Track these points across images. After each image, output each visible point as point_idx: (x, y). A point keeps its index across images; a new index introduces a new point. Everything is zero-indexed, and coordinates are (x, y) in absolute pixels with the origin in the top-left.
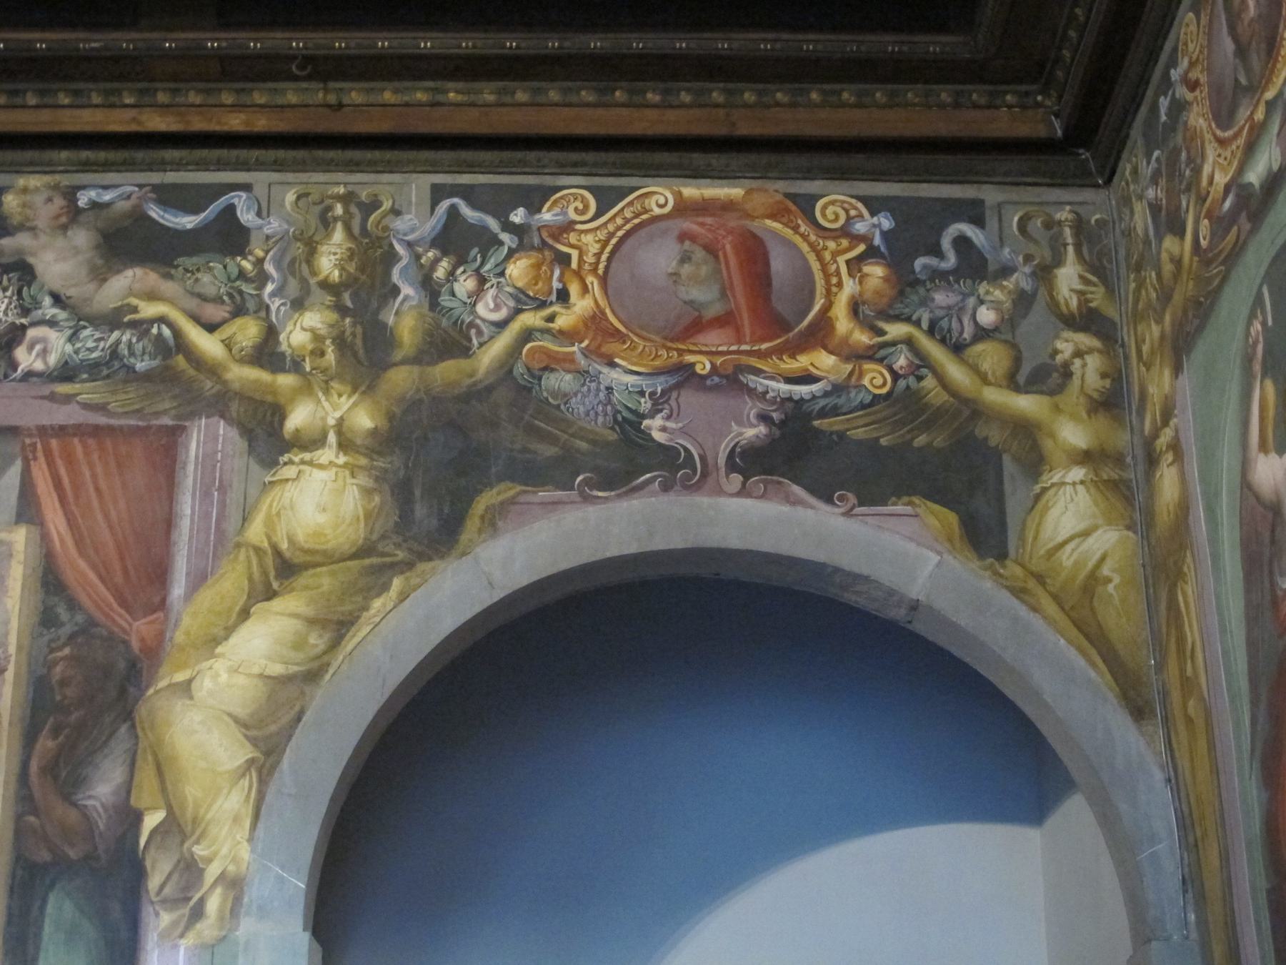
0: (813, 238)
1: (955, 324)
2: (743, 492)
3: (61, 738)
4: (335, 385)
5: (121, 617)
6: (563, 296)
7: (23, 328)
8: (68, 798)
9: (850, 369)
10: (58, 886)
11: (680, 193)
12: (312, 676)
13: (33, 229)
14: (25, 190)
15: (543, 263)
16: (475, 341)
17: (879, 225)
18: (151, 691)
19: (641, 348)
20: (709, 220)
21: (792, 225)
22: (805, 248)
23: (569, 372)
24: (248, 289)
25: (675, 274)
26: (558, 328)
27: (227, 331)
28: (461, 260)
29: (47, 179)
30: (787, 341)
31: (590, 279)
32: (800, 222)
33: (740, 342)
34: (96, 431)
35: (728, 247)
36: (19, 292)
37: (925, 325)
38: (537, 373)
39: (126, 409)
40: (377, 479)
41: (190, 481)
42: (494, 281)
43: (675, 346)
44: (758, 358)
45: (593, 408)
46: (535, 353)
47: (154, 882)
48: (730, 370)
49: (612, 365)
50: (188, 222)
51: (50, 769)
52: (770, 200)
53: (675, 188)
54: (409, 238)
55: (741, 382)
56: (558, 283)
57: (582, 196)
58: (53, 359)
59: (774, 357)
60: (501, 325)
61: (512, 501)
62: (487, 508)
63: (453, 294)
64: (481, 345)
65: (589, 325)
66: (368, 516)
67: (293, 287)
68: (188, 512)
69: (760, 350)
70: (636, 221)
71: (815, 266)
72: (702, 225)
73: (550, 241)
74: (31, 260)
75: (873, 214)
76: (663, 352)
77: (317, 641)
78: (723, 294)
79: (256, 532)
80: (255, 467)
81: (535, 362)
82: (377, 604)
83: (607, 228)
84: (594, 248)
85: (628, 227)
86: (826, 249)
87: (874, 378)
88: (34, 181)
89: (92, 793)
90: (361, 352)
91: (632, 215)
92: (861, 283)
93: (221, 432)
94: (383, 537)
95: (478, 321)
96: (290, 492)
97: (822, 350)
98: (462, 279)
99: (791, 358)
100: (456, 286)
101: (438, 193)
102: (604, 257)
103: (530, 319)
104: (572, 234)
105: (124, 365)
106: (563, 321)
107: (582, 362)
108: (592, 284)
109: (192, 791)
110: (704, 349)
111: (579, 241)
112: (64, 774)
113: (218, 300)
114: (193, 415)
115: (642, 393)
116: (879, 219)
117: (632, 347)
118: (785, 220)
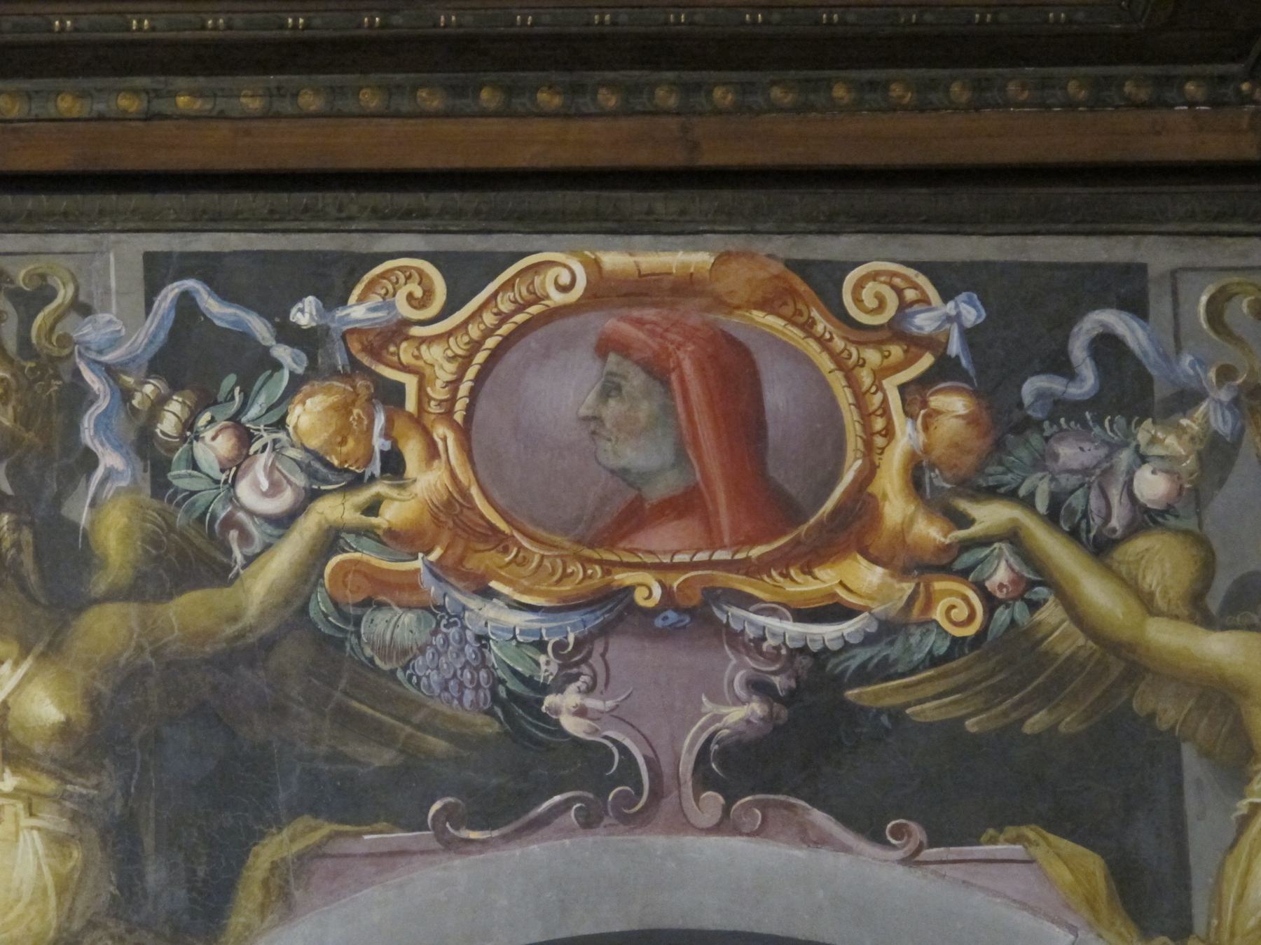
0: (839, 344)
1: (1095, 503)
2: (725, 827)
6: (393, 465)
9: (909, 592)
11: (597, 262)
15: (353, 403)
16: (238, 554)
17: (957, 318)
19: (536, 559)
20: (649, 314)
21: (802, 320)
22: (825, 363)
23: (409, 608)
25: (595, 418)
26: (385, 525)
28: (206, 400)
30: (797, 542)
31: (441, 431)
32: (815, 313)
33: (713, 546)
35: (687, 366)
37: (1042, 504)
38: (351, 611)
40: (74, 818)
42: (267, 438)
43: (596, 556)
44: (747, 574)
45: (455, 676)
46: (346, 575)
48: (696, 598)
49: (487, 594)
52: (762, 274)
53: (587, 253)
54: (108, 358)
55: (718, 621)
56: (382, 440)
57: (421, 273)
59: (774, 573)
60: (284, 522)
61: (316, 853)
62: (274, 866)
63: (195, 466)
64: (249, 560)
65: (443, 518)
66: (62, 888)
69: (748, 558)
70: (520, 318)
71: (844, 397)
72: (639, 323)
73: (365, 360)
75: (946, 297)
76: (576, 568)
78: (681, 456)
81: (348, 592)
83: (467, 333)
84: (446, 372)
85: (505, 329)
86: (863, 366)
87: (953, 607)
90: (33, 579)
91: (512, 307)
92: (926, 428)
94: (91, 925)
95: (241, 515)
97: (859, 557)
98: (208, 434)
99: (804, 573)
100: (199, 450)
102: (464, 388)
104: (404, 345)
106: (391, 515)
107: (432, 589)
108: (445, 439)
110: (649, 559)
111: (418, 357)
115: (541, 646)
116: (957, 306)
117: (520, 559)
118: (788, 310)
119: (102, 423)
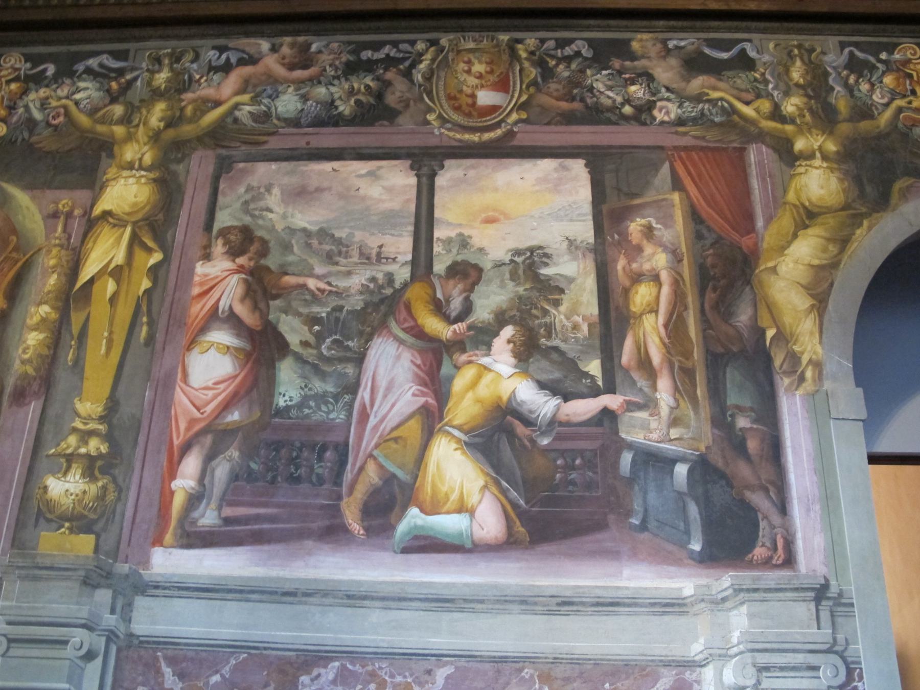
3: (718, 293)
4: (814, 131)
5: (735, 236)
7: (655, 102)
10: (730, 365)
12: (834, 265)
13: (649, 58)
14: (641, 40)
16: (876, 112)
18: (757, 271)
24: (761, 87)
27: (756, 104)
28: (860, 75)
29: (651, 35)
34: (702, 149)
36: (649, 86)
39: (715, 139)
40: (844, 174)
41: (754, 173)
42: (878, 85)
47: (777, 362)
50: (725, 56)
51: (716, 307)
54: (834, 65)
58: (673, 116)
60: (887, 105)
61: (911, 186)
62: (900, 189)
63: (860, 90)
64: (879, 114)
66: (844, 191)
67: (782, 86)
68: (757, 187)
73: (901, 68)
74: (651, 71)
77: (833, 249)
79: (791, 196)
80: (784, 168)
82: (858, 232)
88: (645, 36)
89: (738, 319)
90: (822, 116)
93: (764, 150)
94: (854, 201)
95: (875, 104)
96: (804, 179)
98: (863, 84)
100: (861, 87)
101: (843, 46)
103: (900, 102)
105: (708, 120)
109: (787, 320)
112: (723, 309)
113: (747, 91)
114: (748, 142)
119: (833, 79)
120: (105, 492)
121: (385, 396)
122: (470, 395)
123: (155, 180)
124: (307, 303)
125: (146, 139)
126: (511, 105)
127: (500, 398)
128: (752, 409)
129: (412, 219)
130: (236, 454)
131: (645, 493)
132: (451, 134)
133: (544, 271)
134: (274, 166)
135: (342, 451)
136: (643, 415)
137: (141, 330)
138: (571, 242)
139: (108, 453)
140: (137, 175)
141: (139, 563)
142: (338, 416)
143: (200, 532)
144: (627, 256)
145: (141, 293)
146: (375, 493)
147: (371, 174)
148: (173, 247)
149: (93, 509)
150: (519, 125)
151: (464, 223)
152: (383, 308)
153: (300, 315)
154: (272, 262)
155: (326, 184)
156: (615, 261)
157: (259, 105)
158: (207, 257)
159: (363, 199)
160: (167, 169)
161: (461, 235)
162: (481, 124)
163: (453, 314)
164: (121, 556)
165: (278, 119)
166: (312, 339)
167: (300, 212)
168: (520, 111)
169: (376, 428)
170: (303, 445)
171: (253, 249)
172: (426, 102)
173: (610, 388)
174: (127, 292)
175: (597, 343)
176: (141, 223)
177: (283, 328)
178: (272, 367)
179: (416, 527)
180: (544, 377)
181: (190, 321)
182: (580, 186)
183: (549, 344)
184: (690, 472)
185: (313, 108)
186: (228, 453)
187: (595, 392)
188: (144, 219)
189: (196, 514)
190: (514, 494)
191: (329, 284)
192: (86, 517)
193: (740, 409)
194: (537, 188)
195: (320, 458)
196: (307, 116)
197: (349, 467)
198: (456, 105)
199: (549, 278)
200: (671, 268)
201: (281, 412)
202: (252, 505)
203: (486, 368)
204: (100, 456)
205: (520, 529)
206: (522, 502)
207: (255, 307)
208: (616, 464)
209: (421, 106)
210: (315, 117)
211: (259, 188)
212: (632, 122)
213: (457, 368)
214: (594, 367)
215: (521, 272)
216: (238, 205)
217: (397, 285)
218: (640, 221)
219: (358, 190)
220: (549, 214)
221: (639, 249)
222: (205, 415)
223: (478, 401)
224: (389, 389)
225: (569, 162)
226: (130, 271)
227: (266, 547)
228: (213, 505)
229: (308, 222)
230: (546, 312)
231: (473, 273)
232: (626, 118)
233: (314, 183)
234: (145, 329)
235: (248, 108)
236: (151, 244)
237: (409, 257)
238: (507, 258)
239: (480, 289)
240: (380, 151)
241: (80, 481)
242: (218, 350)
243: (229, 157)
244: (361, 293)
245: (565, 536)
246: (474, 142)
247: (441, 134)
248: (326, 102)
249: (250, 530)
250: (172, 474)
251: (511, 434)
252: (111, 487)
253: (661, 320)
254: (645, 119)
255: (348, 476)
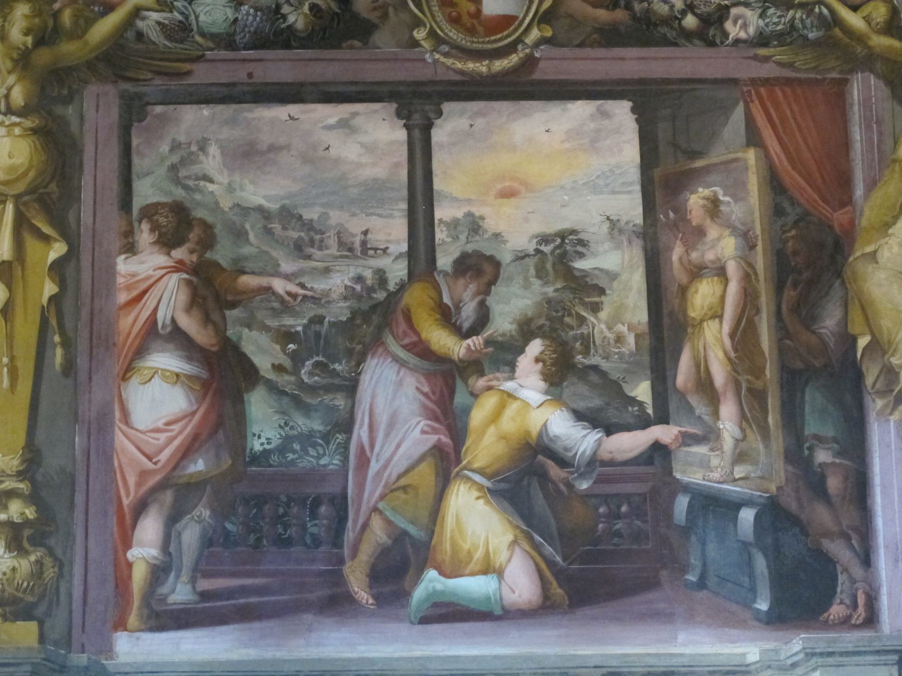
3: (799, 289)
5: (826, 210)
8: (808, 328)
10: (811, 384)
18: (851, 259)
34: (789, 82)
39: (807, 67)
41: (856, 117)
47: (869, 381)
51: (796, 309)
58: (751, 30)
68: (859, 138)
89: (823, 325)
93: (872, 83)
105: (801, 35)
112: (804, 313)
114: (851, 71)
120: (41, 568)
121: (387, 434)
122: (492, 430)
123: (35, 131)
124: (276, 313)
125: (9, 64)
126: (531, 15)
127: (528, 433)
128: (835, 440)
129: (405, 193)
130: (206, 513)
131: (704, 544)
132: (449, 62)
133: (580, 265)
134: (206, 111)
135: (340, 504)
136: (701, 450)
137: (55, 354)
138: (613, 224)
139: (37, 519)
140: (7, 123)
141: (101, 652)
142: (330, 461)
143: (172, 611)
144: (685, 243)
145: (45, 301)
146: (384, 553)
147: (344, 124)
148: (79, 235)
149: (30, 590)
150: (542, 47)
151: (473, 198)
152: (376, 319)
153: (267, 329)
154: (222, 254)
155: (282, 140)
156: (670, 249)
157: (171, 12)
158: (130, 249)
159: (337, 161)
160: (50, 113)
161: (469, 214)
162: (489, 46)
163: (466, 325)
164: (75, 645)
165: (203, 35)
166: (287, 363)
167: (252, 182)
168: (543, 26)
169: (379, 474)
170: (290, 499)
171: (193, 236)
172: (411, 11)
173: (663, 418)
174: (25, 300)
175: (646, 359)
176: (26, 198)
177: (248, 348)
178: (239, 401)
179: (435, 592)
180: (581, 405)
181: (122, 338)
182: (624, 142)
183: (587, 362)
184: (757, 518)
185: (251, 18)
186: (196, 513)
187: (644, 423)
188: (31, 191)
189: (164, 590)
190: (549, 550)
191: (302, 286)
192: (22, 600)
193: (818, 438)
194: (567, 145)
195: (314, 515)
196: (243, 31)
197: (350, 524)
198: (454, 14)
199: (585, 274)
200: (741, 258)
201: (258, 459)
202: (233, 575)
203: (511, 396)
204: (27, 523)
205: (557, 591)
206: (558, 559)
207: (207, 320)
208: (668, 513)
209: (404, 16)
210: (255, 32)
211: (190, 144)
212: (696, 41)
213: (475, 395)
214: (642, 391)
215: (549, 266)
216: (162, 171)
217: (392, 287)
218: (704, 192)
219: (327, 149)
220: (584, 184)
221: (700, 232)
222: (160, 465)
223: (503, 437)
224: (391, 425)
225: (610, 105)
226: (23, 270)
227: (257, 625)
228: (184, 578)
229: (264, 197)
230: (582, 320)
231: (488, 268)
232: (688, 35)
233: (265, 139)
234: (59, 352)
235: (155, 16)
236: (47, 229)
237: (404, 247)
238: (531, 248)
239: (498, 290)
240: (353, 88)
241: (6, 556)
242: (164, 378)
243: (139, 96)
244: (345, 298)
245: (612, 596)
246: (480, 74)
247: (436, 61)
248: (269, 8)
249: (234, 605)
250: (127, 543)
251: (543, 476)
252: (48, 561)
253: (726, 328)
254: (713, 36)
255: (350, 535)
